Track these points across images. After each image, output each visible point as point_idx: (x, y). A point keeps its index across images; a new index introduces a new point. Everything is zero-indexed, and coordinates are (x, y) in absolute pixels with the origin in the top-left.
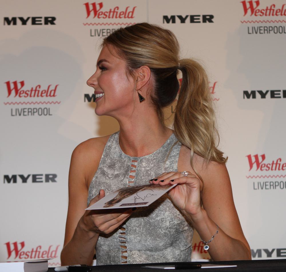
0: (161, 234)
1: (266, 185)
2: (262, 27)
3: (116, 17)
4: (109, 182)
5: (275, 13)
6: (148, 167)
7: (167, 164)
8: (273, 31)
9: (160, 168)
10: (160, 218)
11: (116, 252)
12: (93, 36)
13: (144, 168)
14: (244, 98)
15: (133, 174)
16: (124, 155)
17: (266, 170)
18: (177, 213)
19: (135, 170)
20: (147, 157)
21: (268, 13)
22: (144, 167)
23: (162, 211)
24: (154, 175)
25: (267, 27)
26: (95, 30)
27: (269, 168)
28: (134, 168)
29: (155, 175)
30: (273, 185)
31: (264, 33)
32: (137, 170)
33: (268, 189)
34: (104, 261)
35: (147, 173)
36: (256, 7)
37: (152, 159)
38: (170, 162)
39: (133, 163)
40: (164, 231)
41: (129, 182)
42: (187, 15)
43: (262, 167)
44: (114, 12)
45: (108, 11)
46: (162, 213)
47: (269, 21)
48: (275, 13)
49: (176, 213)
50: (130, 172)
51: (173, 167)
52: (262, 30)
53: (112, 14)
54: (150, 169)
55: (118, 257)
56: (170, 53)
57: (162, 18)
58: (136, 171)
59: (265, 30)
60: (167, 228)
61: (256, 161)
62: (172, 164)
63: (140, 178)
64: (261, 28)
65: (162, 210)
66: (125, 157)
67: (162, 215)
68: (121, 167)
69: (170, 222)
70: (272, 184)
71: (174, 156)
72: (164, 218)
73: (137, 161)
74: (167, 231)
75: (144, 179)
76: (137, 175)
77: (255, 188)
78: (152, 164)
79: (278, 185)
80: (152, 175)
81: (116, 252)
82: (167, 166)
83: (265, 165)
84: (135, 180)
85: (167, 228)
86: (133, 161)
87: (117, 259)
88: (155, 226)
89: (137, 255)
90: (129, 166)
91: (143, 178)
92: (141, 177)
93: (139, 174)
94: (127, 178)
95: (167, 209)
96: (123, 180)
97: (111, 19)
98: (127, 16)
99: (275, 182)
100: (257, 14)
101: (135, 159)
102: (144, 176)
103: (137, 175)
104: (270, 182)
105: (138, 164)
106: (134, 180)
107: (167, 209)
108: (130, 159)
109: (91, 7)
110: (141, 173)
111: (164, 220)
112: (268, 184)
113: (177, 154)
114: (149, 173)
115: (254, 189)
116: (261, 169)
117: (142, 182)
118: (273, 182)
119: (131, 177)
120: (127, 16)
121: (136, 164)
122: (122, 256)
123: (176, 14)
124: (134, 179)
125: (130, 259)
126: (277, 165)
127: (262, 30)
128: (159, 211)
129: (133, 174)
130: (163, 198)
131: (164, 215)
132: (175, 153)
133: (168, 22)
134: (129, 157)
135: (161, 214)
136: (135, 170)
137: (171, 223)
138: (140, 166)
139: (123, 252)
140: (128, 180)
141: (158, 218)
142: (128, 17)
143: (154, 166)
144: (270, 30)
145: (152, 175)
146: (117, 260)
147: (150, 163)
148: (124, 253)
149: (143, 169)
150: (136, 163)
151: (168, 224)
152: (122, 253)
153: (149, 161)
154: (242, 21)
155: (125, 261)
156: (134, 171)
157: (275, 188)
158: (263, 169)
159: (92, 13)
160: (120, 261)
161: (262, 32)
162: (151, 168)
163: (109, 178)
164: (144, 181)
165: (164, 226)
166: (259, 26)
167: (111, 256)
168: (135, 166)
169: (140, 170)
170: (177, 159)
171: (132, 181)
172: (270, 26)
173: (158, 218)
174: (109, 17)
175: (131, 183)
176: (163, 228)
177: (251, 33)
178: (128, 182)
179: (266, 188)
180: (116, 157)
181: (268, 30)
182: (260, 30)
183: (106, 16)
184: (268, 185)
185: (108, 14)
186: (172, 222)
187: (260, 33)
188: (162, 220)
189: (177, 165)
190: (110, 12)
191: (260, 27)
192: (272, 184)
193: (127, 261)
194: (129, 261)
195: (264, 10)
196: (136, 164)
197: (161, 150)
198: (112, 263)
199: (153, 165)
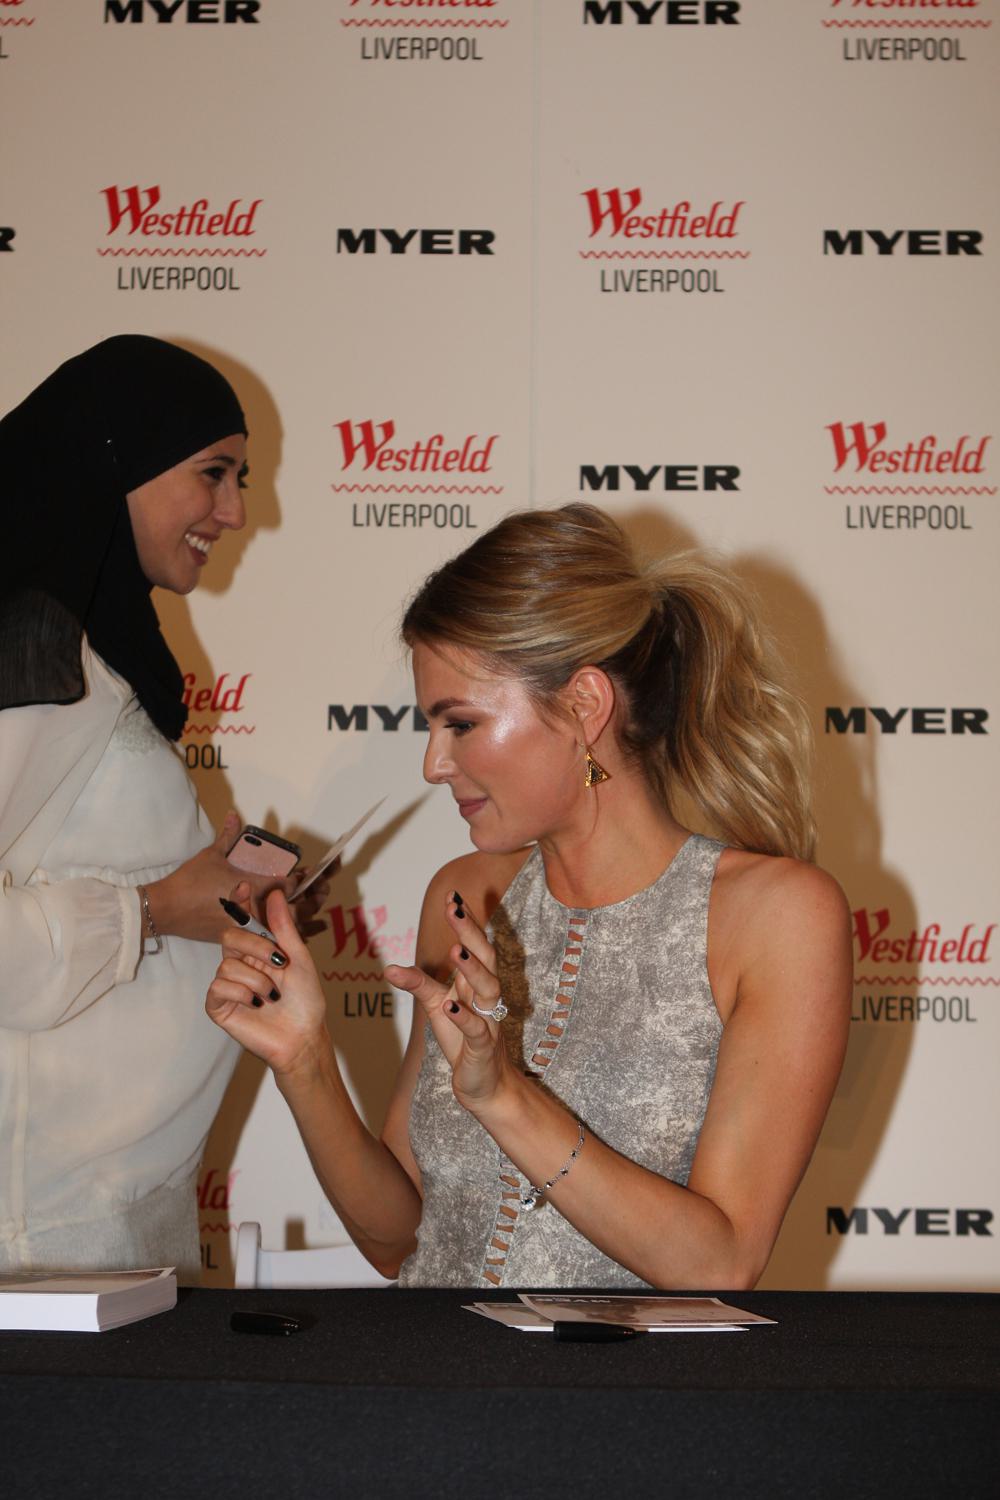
0: (635, 1153)
2: (891, 507)
4: (505, 975)
5: (933, 465)
6: (618, 944)
7: (675, 935)
8: (925, 522)
9: (654, 949)
11: (485, 1190)
13: (604, 947)
15: (574, 960)
16: (549, 900)
18: (697, 1093)
19: (580, 949)
20: (610, 910)
21: (912, 464)
22: (606, 944)
23: (650, 1081)
24: (635, 969)
25: (907, 508)
28: (575, 942)
29: (638, 970)
32: (585, 948)
34: (442, 1213)
35: (614, 961)
36: (875, 446)
37: (624, 921)
38: (683, 929)
39: (574, 927)
40: (646, 1146)
41: (562, 984)
42: (657, 464)
44: (428, 451)
45: (411, 447)
46: (650, 1086)
47: (889, 490)
48: (933, 465)
49: (693, 1092)
50: (566, 954)
51: (693, 947)
52: (891, 516)
53: (421, 457)
54: (624, 952)
55: (488, 1207)
56: (631, 585)
57: (577, 473)
58: (583, 951)
59: (900, 517)
62: (692, 937)
63: (593, 975)
64: (889, 512)
65: (650, 1077)
66: (552, 907)
67: (648, 1094)
68: (541, 935)
71: (694, 910)
72: (650, 1105)
73: (583, 923)
75: (604, 978)
76: (586, 962)
78: (628, 936)
80: (631, 970)
81: (485, 1190)
82: (675, 941)
84: (579, 978)
85: (659, 1138)
86: (572, 921)
87: (485, 1212)
88: (620, 1124)
89: (549, 1215)
90: (562, 935)
91: (601, 976)
92: (597, 973)
93: (591, 960)
94: (557, 971)
95: (668, 1077)
96: (545, 975)
97: (418, 473)
98: (467, 464)
100: (877, 466)
101: (579, 916)
102: (605, 971)
103: (586, 962)
105: (589, 932)
106: (574, 978)
107: (668, 1077)
108: (564, 916)
109: (357, 436)
110: (596, 961)
111: (650, 1110)
113: (704, 906)
114: (621, 961)
117: (600, 988)
119: (569, 969)
120: (467, 464)
121: (581, 930)
122: (501, 1207)
123: (620, 460)
124: (574, 976)
125: (523, 1223)
127: (891, 516)
128: (638, 1081)
129: (574, 960)
130: (661, 1039)
131: (654, 1094)
132: (695, 901)
133: (596, 484)
134: (561, 908)
135: (644, 1089)
136: (580, 949)
138: (595, 939)
139: (505, 1196)
140: (559, 976)
142: (471, 468)
143: (635, 942)
144: (916, 518)
145: (631, 970)
146: (483, 1215)
147: (623, 931)
148: (510, 1200)
149: (603, 949)
150: (581, 926)
151: (662, 1125)
152: (504, 1198)
153: (618, 924)
154: (830, 488)
155: (509, 1224)
156: (577, 951)
159: (361, 455)
160: (493, 1220)
162: (625, 947)
163: (509, 965)
164: (606, 984)
165: (648, 1128)
166: (882, 504)
167: (470, 1202)
168: (578, 938)
169: (594, 951)
170: (704, 923)
171: (570, 980)
172: (916, 504)
174: (413, 468)
175: (565, 988)
178: (557, 984)
180: (533, 906)
181: (911, 517)
182: (885, 516)
183: (404, 462)
185: (409, 459)
187: (885, 527)
188: (645, 1110)
189: (705, 941)
190: (417, 450)
191: (885, 507)
193: (512, 1227)
194: (520, 1227)
195: (899, 454)
196: (581, 930)
197: (652, 895)
198: (464, 1221)
199: (630, 941)
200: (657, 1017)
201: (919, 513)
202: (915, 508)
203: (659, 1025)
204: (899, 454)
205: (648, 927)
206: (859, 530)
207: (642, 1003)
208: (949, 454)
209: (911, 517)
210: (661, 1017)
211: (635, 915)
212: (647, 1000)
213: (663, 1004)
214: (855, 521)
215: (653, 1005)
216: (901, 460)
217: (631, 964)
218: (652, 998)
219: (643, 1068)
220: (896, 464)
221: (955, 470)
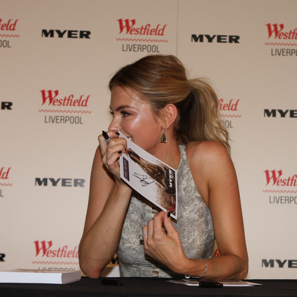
1: (281, 200)
3: (147, 34)
12: (125, 51)
14: (265, 116)
17: (282, 185)
25: (290, 50)
26: (127, 45)
27: (285, 183)
30: (288, 200)
31: (287, 55)
33: (283, 203)
42: (215, 34)
43: (278, 182)
44: (145, 29)
61: (272, 177)
70: (287, 198)
77: (271, 201)
79: (293, 200)
83: (281, 180)
99: (290, 197)
100: (281, 37)
104: (286, 197)
112: (284, 198)
115: (270, 202)
116: (278, 185)
118: (288, 197)
126: (292, 181)
142: (159, 34)
144: (292, 53)
154: (267, 43)
157: (290, 203)
158: (279, 184)
161: (284, 54)
177: (274, 55)
179: (281, 203)
181: (291, 53)
184: (283, 200)
185: (140, 31)
192: (287, 198)
200: (186, 212)
202: (292, 50)
203: (188, 214)
204: (287, 33)
209: (291, 53)
210: (188, 212)
213: (187, 207)
215: (184, 209)
218: (183, 207)
220: (286, 36)
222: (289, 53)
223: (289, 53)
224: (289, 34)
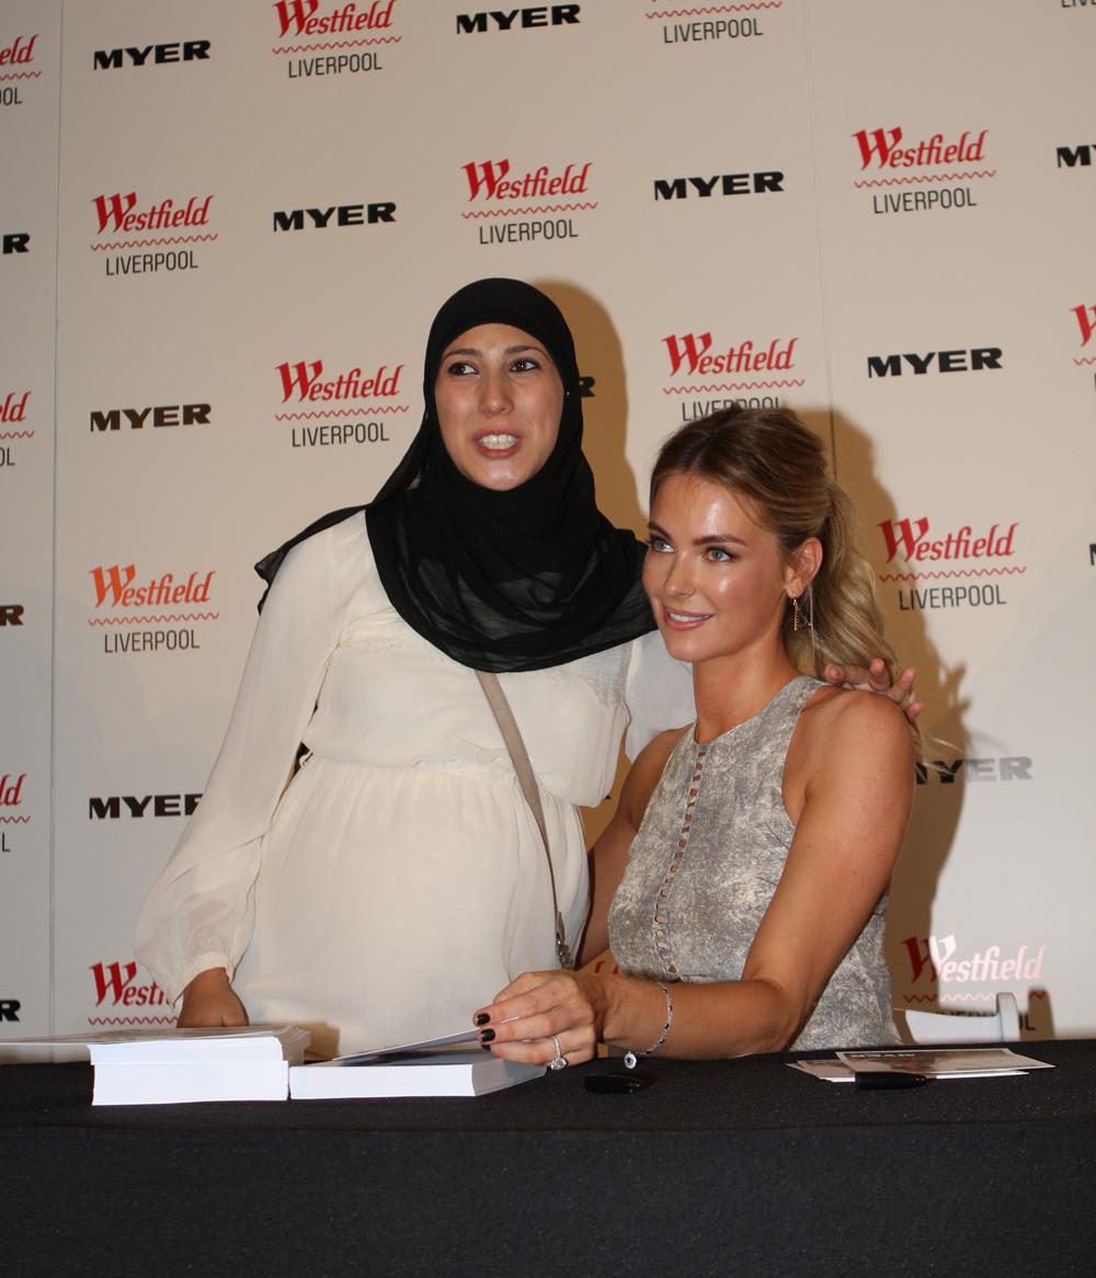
10: (730, 883)
60: (750, 908)
69: (756, 893)
74: (749, 917)
137: (759, 895)
141: (726, 885)
143: (737, 762)
161: (909, 206)
173: (726, 885)
176: (738, 907)
186: (763, 894)
187: (906, 210)
201: (933, 196)
202: (929, 193)
205: (747, 749)
206: (885, 214)
207: (734, 807)
208: (955, 147)
211: (738, 740)
212: (738, 805)
214: (881, 207)
215: (742, 809)
216: (916, 156)
217: (732, 779)
219: (734, 857)
221: (960, 160)
222: (923, 201)
223: (923, 201)
224: (918, 152)
